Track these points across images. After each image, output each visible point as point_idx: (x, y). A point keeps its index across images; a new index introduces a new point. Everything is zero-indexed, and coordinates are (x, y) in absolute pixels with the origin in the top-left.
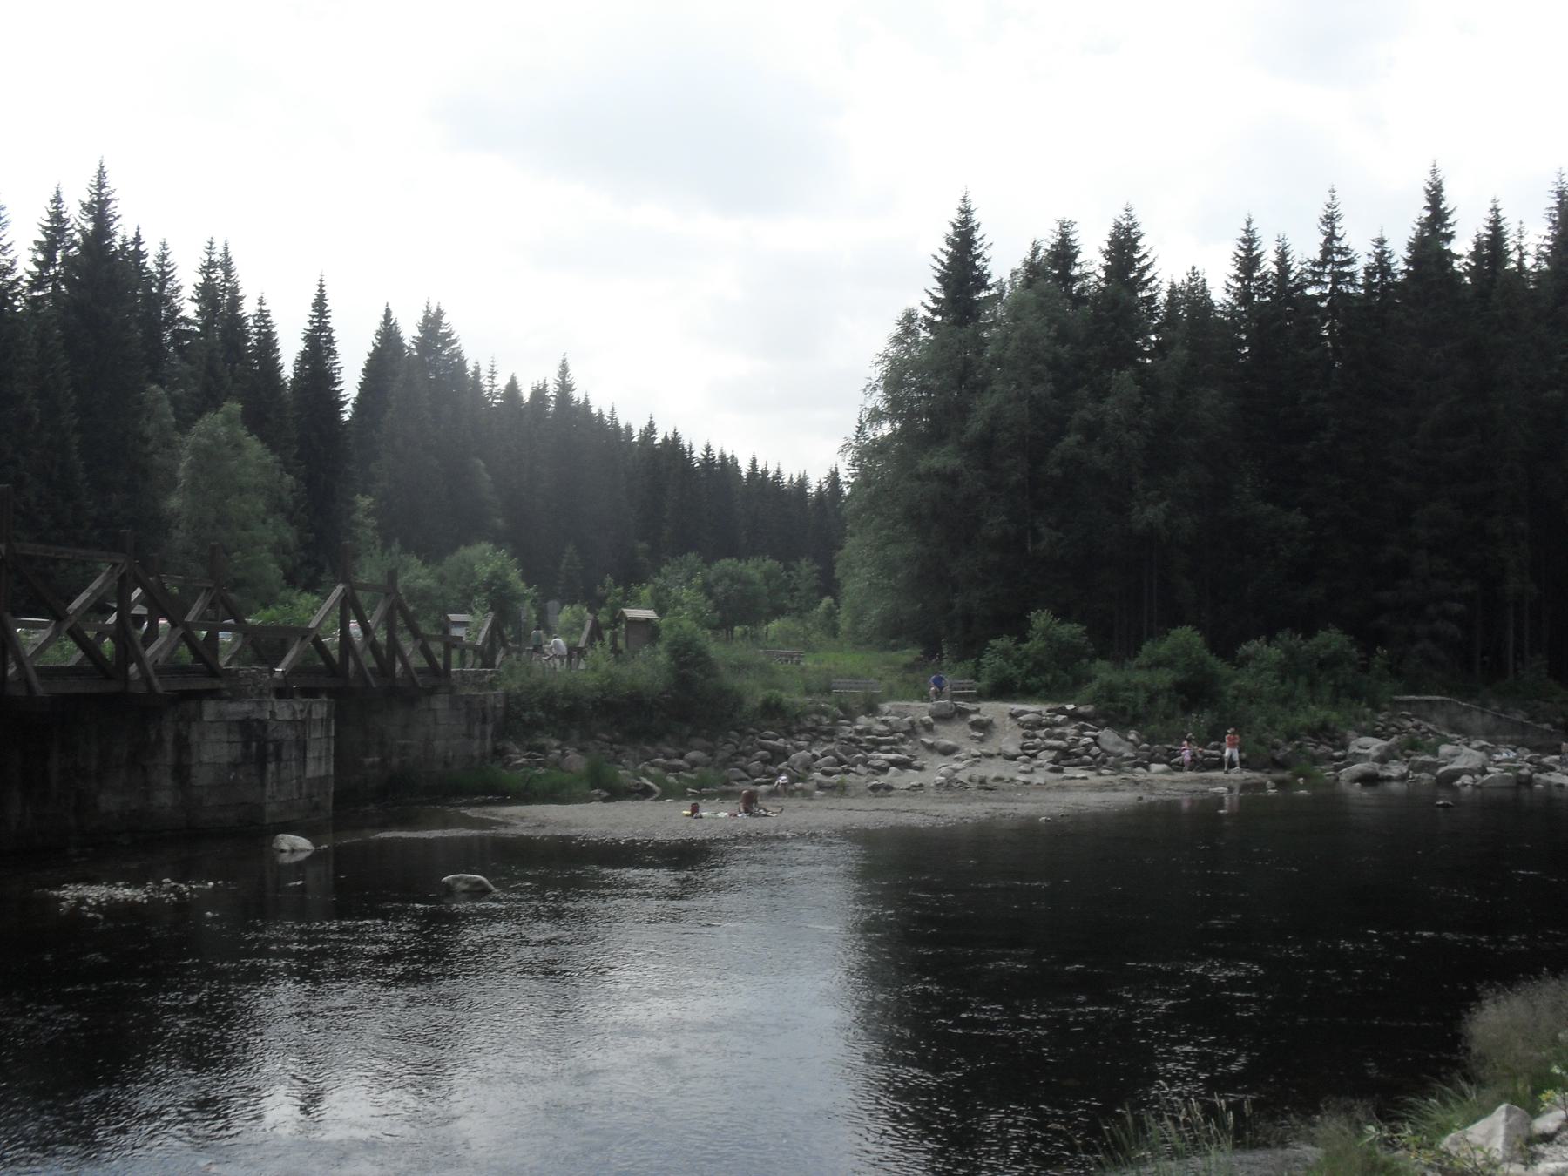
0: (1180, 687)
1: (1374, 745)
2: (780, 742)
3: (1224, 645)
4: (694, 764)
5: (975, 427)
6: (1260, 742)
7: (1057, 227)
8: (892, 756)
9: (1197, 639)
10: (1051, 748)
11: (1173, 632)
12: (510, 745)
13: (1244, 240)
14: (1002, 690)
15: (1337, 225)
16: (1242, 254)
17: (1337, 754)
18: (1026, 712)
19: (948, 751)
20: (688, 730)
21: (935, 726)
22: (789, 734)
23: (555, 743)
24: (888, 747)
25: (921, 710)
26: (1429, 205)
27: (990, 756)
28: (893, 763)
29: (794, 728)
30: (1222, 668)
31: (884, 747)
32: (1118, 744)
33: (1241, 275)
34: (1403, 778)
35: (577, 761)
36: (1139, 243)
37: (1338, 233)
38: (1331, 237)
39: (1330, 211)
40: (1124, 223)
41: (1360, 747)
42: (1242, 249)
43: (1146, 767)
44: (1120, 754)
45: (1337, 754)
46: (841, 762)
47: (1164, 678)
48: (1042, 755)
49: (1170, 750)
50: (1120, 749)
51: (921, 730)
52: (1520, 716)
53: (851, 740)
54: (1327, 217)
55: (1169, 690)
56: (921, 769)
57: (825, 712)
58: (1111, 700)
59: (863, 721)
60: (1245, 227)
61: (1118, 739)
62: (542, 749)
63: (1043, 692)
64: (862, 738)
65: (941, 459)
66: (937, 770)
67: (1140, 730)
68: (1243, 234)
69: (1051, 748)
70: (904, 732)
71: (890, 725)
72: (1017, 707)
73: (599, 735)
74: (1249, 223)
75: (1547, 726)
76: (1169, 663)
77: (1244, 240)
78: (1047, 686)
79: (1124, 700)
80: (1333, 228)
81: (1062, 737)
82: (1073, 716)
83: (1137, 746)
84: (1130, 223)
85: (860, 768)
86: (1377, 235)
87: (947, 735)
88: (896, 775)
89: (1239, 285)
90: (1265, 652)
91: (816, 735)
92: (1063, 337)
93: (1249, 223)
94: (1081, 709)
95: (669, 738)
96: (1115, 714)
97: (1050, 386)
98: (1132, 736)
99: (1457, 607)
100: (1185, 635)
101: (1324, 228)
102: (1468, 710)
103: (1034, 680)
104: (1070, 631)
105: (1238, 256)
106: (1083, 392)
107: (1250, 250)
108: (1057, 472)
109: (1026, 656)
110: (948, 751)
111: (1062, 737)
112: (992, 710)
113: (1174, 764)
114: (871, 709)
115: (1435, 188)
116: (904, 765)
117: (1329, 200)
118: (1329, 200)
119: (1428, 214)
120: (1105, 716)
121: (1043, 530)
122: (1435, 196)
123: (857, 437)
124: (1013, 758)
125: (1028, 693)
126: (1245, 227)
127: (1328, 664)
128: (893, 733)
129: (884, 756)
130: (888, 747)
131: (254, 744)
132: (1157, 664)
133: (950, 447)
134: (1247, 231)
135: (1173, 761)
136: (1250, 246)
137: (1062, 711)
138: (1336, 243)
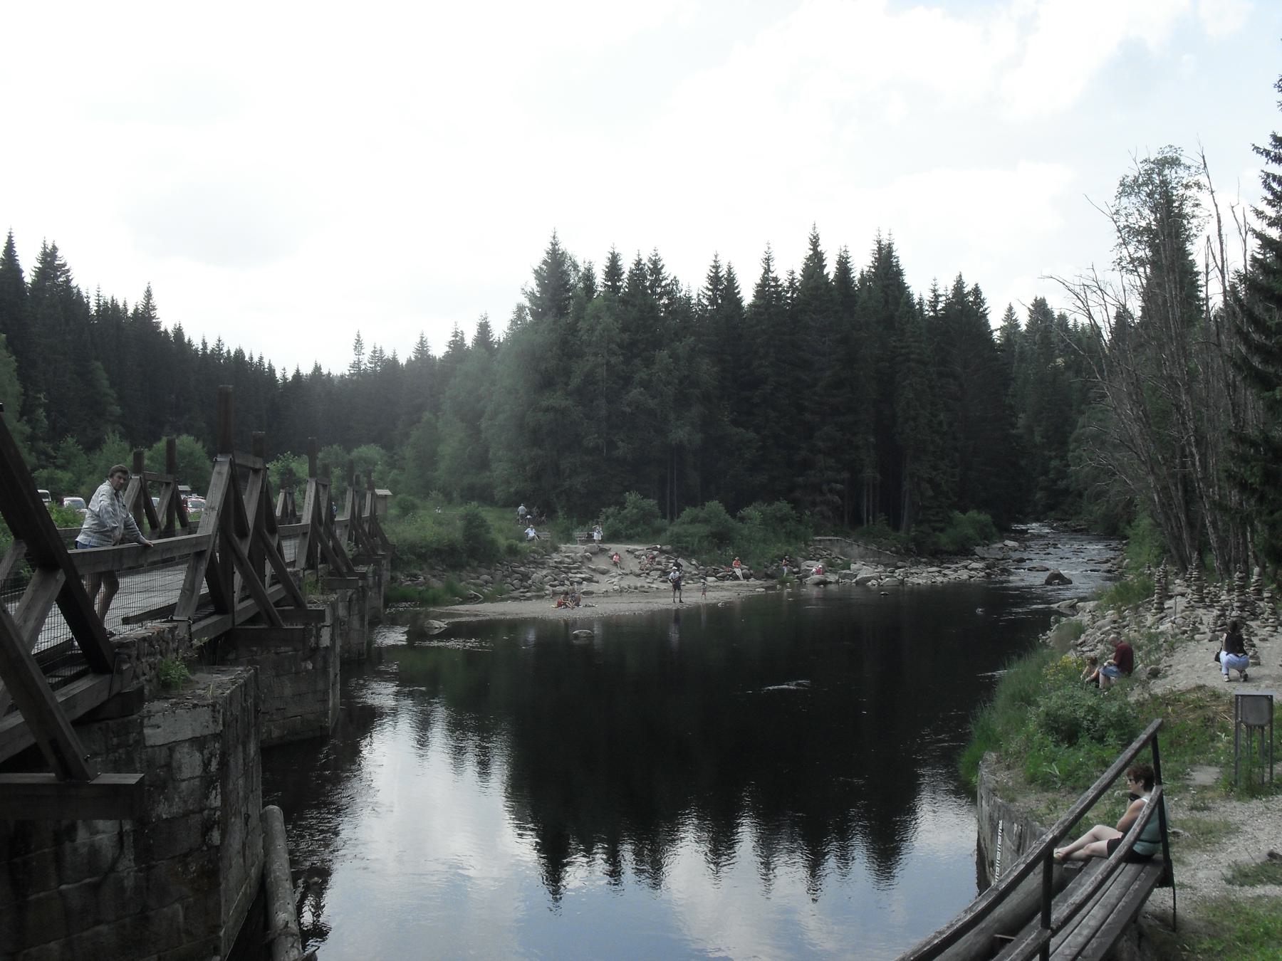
0: (714, 535)
1: (816, 566)
2: (522, 569)
3: (733, 509)
4: (487, 582)
5: (576, 381)
6: (759, 564)
7: (610, 256)
8: (583, 576)
9: (721, 508)
10: (657, 570)
11: (707, 504)
12: (399, 574)
13: (713, 267)
14: (612, 537)
15: (771, 264)
16: (712, 274)
17: (795, 570)
18: (637, 550)
19: (604, 573)
20: (476, 564)
21: (593, 559)
22: (524, 565)
23: (420, 573)
24: (575, 571)
25: (580, 549)
26: (812, 247)
27: (627, 574)
28: (584, 579)
29: (525, 561)
30: (732, 522)
31: (573, 571)
32: (688, 567)
33: (710, 287)
34: (837, 582)
35: (437, 584)
36: (663, 271)
37: (772, 269)
38: (767, 271)
39: (767, 255)
40: (654, 258)
41: (808, 566)
42: (712, 272)
43: (705, 579)
44: (690, 573)
45: (795, 570)
46: (555, 580)
47: (703, 529)
48: (652, 573)
49: (715, 569)
50: (689, 570)
51: (585, 560)
52: (874, 547)
53: (556, 567)
54: (766, 259)
55: (708, 536)
56: (597, 582)
57: (534, 552)
58: (678, 542)
59: (556, 557)
60: (714, 259)
61: (688, 564)
62: (415, 576)
63: (637, 537)
64: (561, 566)
65: (556, 399)
66: (604, 584)
67: (697, 560)
68: (713, 264)
69: (657, 570)
70: (580, 562)
71: (572, 558)
72: (631, 547)
73: (437, 567)
74: (716, 256)
75: (888, 552)
76: (706, 521)
77: (713, 267)
78: (638, 535)
79: (687, 542)
80: (769, 266)
81: (659, 563)
82: (662, 552)
83: (697, 568)
84: (657, 258)
85: (566, 582)
86: (790, 268)
87: (601, 563)
88: (587, 586)
89: (710, 293)
90: (753, 512)
91: (540, 564)
92: (624, 329)
93: (716, 256)
94: (664, 548)
95: (468, 568)
96: (682, 549)
97: (621, 358)
98: (694, 562)
99: (839, 486)
100: (715, 506)
101: (764, 265)
102: (851, 545)
103: (632, 531)
104: (651, 503)
105: (709, 276)
106: (638, 361)
107: (717, 273)
108: (628, 410)
109: (626, 518)
110: (604, 573)
111: (659, 563)
112: (617, 548)
113: (719, 577)
114: (556, 550)
115: (814, 237)
116: (590, 580)
117: (766, 250)
118: (766, 250)
119: (811, 252)
120: (677, 552)
121: (620, 444)
122: (815, 243)
123: (356, 347)
124: (639, 575)
125: (629, 539)
126: (714, 259)
127: (782, 520)
128: (574, 563)
129: (579, 575)
130: (575, 571)
131: (377, 577)
132: (693, 521)
133: (559, 393)
134: (715, 261)
135: (718, 575)
136: (717, 271)
137: (655, 549)
138: (771, 275)
